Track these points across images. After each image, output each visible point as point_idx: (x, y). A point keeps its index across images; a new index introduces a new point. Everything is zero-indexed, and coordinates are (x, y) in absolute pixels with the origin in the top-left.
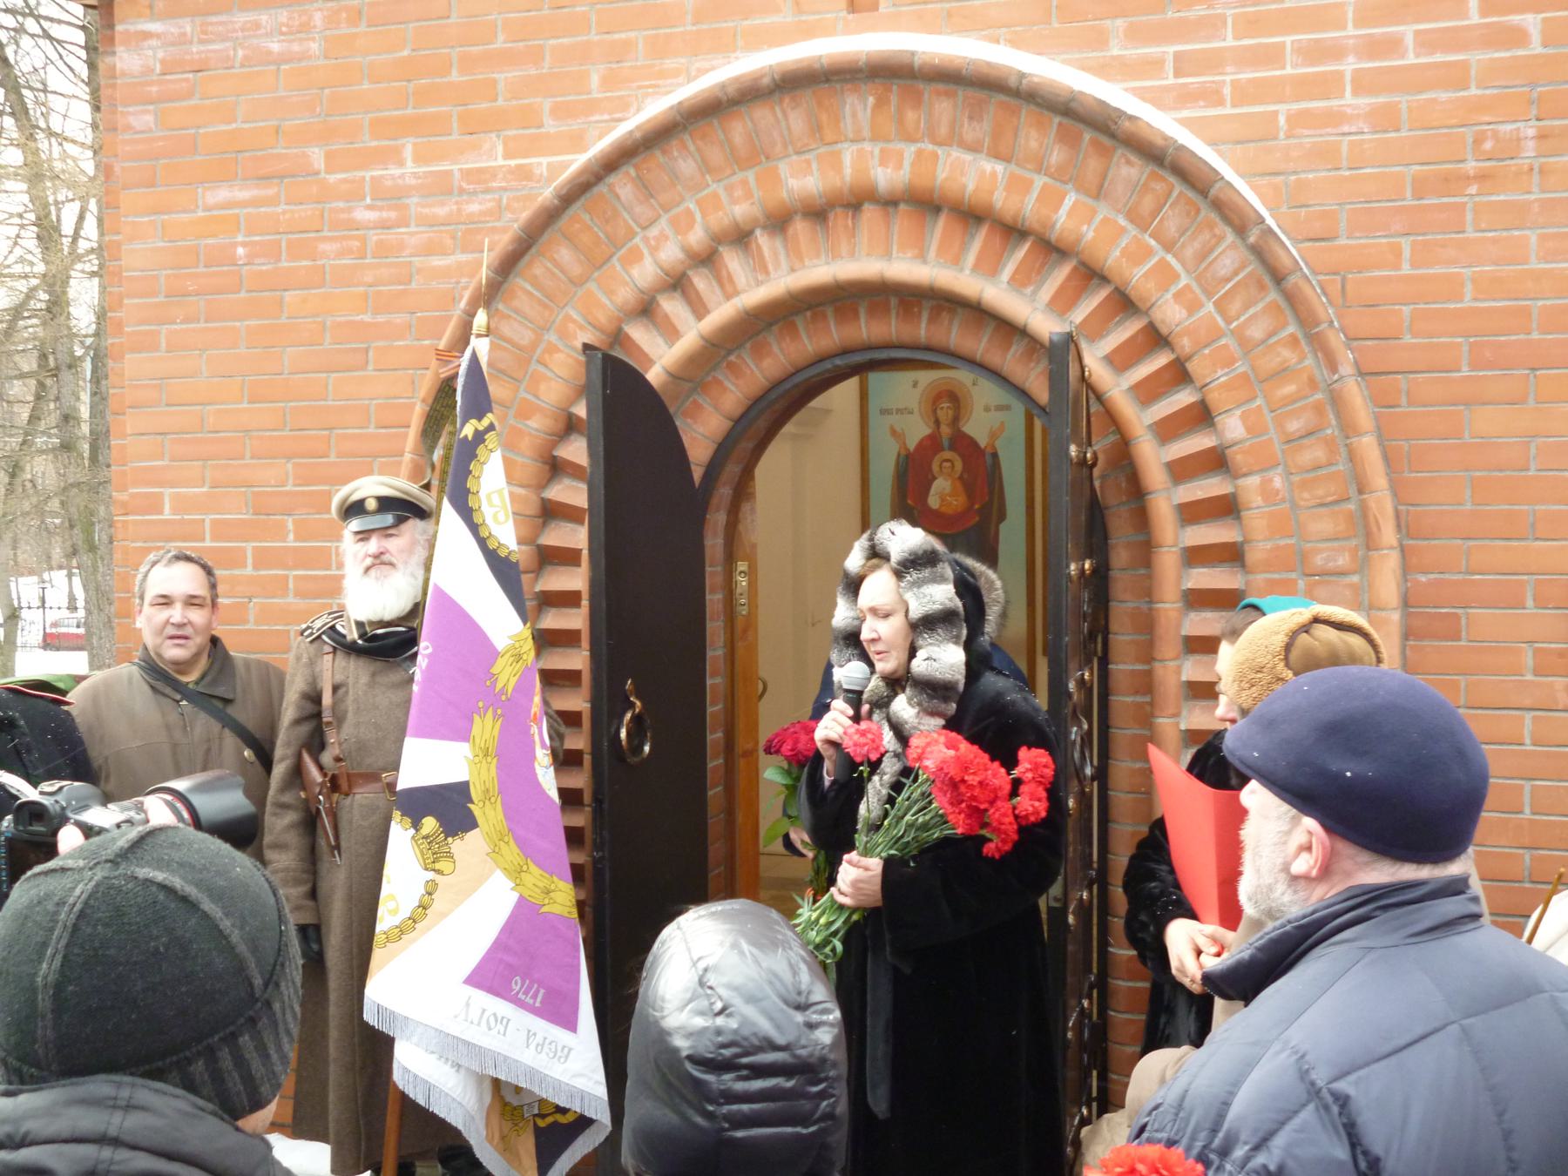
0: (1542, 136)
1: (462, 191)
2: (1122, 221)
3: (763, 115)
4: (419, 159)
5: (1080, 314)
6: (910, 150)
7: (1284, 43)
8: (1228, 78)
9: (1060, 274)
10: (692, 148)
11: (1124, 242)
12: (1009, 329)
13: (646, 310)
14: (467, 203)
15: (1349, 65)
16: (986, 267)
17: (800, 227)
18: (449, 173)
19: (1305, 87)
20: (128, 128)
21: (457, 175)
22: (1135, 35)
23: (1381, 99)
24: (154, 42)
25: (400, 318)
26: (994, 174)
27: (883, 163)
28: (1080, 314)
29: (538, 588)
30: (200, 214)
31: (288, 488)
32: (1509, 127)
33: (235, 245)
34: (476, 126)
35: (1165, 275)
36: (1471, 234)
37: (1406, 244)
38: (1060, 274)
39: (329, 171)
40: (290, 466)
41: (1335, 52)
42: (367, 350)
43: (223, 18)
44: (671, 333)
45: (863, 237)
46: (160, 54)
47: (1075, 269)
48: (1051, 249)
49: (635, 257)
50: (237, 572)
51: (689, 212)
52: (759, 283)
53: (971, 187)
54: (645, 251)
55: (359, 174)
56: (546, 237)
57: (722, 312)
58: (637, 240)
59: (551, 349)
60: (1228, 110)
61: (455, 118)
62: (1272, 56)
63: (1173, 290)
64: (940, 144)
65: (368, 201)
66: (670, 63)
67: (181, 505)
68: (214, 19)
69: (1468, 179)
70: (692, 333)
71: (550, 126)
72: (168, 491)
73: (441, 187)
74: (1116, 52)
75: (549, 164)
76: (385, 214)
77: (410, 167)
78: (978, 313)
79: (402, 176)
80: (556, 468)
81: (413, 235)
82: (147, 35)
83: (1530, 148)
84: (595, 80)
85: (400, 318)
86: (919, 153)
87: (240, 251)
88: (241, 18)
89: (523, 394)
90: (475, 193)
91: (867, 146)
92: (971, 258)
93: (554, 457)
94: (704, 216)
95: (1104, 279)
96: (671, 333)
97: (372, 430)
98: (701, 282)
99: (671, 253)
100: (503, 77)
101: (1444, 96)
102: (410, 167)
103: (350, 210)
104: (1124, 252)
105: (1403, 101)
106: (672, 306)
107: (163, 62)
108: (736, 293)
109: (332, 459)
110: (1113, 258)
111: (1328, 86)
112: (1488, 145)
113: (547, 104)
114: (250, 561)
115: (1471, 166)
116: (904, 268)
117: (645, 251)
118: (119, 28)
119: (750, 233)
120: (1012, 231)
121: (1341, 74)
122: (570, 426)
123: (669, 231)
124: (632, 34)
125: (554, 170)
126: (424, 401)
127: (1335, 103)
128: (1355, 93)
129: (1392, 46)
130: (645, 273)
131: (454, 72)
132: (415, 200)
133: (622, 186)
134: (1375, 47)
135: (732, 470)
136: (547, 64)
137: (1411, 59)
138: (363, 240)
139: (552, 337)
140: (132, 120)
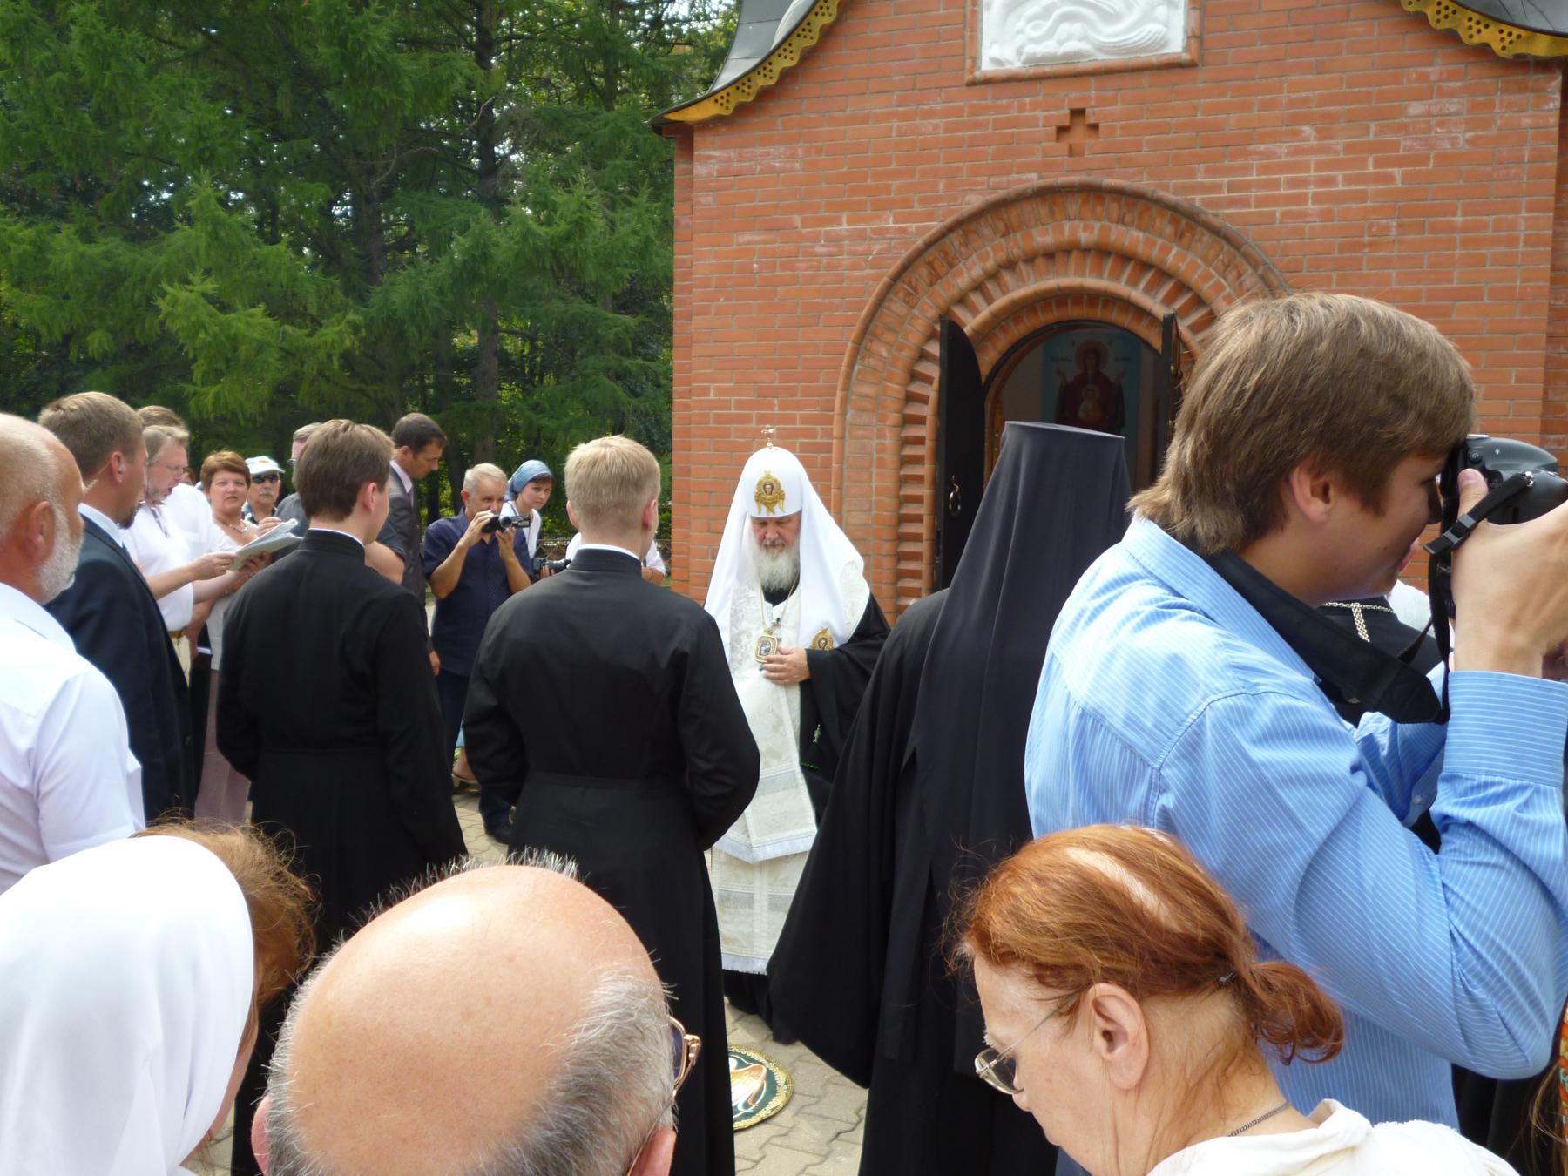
0: (1400, 226)
1: (871, 239)
2: (1199, 261)
3: (1027, 209)
4: (850, 222)
5: (1177, 305)
6: (1097, 225)
7: (1280, 179)
8: (1253, 194)
9: (1168, 287)
10: (990, 220)
11: (1200, 271)
12: (1142, 313)
13: (962, 300)
14: (874, 244)
15: (1311, 190)
16: (1133, 282)
17: (1040, 261)
18: (865, 230)
19: (1290, 200)
20: (699, 203)
21: (869, 230)
22: (1210, 172)
23: (1325, 206)
24: (713, 161)
25: (836, 301)
26: (1138, 237)
27: (1084, 231)
28: (1177, 305)
29: (902, 435)
30: (735, 247)
31: (777, 384)
32: (1384, 221)
33: (753, 263)
34: (879, 207)
35: (1219, 288)
36: (1364, 271)
37: (1334, 275)
38: (1168, 287)
39: (803, 227)
40: (777, 373)
41: (1304, 183)
42: (819, 318)
43: (751, 149)
44: (974, 311)
45: (1072, 266)
46: (717, 167)
47: (1175, 284)
48: (1163, 274)
49: (960, 273)
50: (747, 426)
51: (987, 252)
52: (1019, 287)
53: (1127, 243)
54: (964, 270)
56: (916, 263)
57: (1000, 302)
58: (961, 265)
59: (915, 317)
60: (1253, 210)
61: (869, 203)
63: (1223, 294)
64: (1111, 222)
65: (823, 242)
66: (979, 179)
67: (719, 391)
68: (746, 150)
69: (1362, 245)
70: (985, 312)
71: (917, 208)
72: (713, 386)
73: (861, 236)
74: (1199, 180)
75: (916, 227)
76: (831, 249)
77: (845, 227)
78: (1127, 305)
79: (841, 230)
80: (914, 376)
81: (845, 259)
82: (710, 157)
83: (1394, 232)
84: (941, 186)
85: (836, 301)
86: (1102, 228)
87: (755, 266)
88: (760, 150)
89: (900, 339)
90: (877, 239)
91: (1077, 222)
92: (1125, 277)
93: (913, 371)
94: (995, 254)
95: (1189, 289)
96: (974, 311)
97: (820, 356)
98: (991, 287)
99: (977, 272)
100: (895, 184)
101: (1355, 205)
102: (845, 227)
103: (812, 247)
104: (1199, 276)
105: (1336, 207)
106: (976, 298)
107: (718, 171)
108: (1008, 292)
109: (799, 370)
110: (1194, 279)
111: (1301, 199)
112: (1374, 229)
113: (916, 197)
114: (754, 419)
115: (1366, 238)
116: (1091, 282)
117: (964, 270)
118: (696, 153)
119: (1017, 262)
120: (1145, 266)
121: (1306, 195)
122: (923, 356)
123: (977, 261)
124: (961, 164)
125: (920, 231)
126: (853, 342)
127: (1303, 208)
128: (1314, 203)
129: (1331, 181)
130: (963, 282)
131: (869, 180)
132: (847, 242)
133: (955, 240)
135: (997, 380)
136: (917, 177)
137: (1340, 188)
138: (819, 262)
139: (916, 311)
140: (702, 200)
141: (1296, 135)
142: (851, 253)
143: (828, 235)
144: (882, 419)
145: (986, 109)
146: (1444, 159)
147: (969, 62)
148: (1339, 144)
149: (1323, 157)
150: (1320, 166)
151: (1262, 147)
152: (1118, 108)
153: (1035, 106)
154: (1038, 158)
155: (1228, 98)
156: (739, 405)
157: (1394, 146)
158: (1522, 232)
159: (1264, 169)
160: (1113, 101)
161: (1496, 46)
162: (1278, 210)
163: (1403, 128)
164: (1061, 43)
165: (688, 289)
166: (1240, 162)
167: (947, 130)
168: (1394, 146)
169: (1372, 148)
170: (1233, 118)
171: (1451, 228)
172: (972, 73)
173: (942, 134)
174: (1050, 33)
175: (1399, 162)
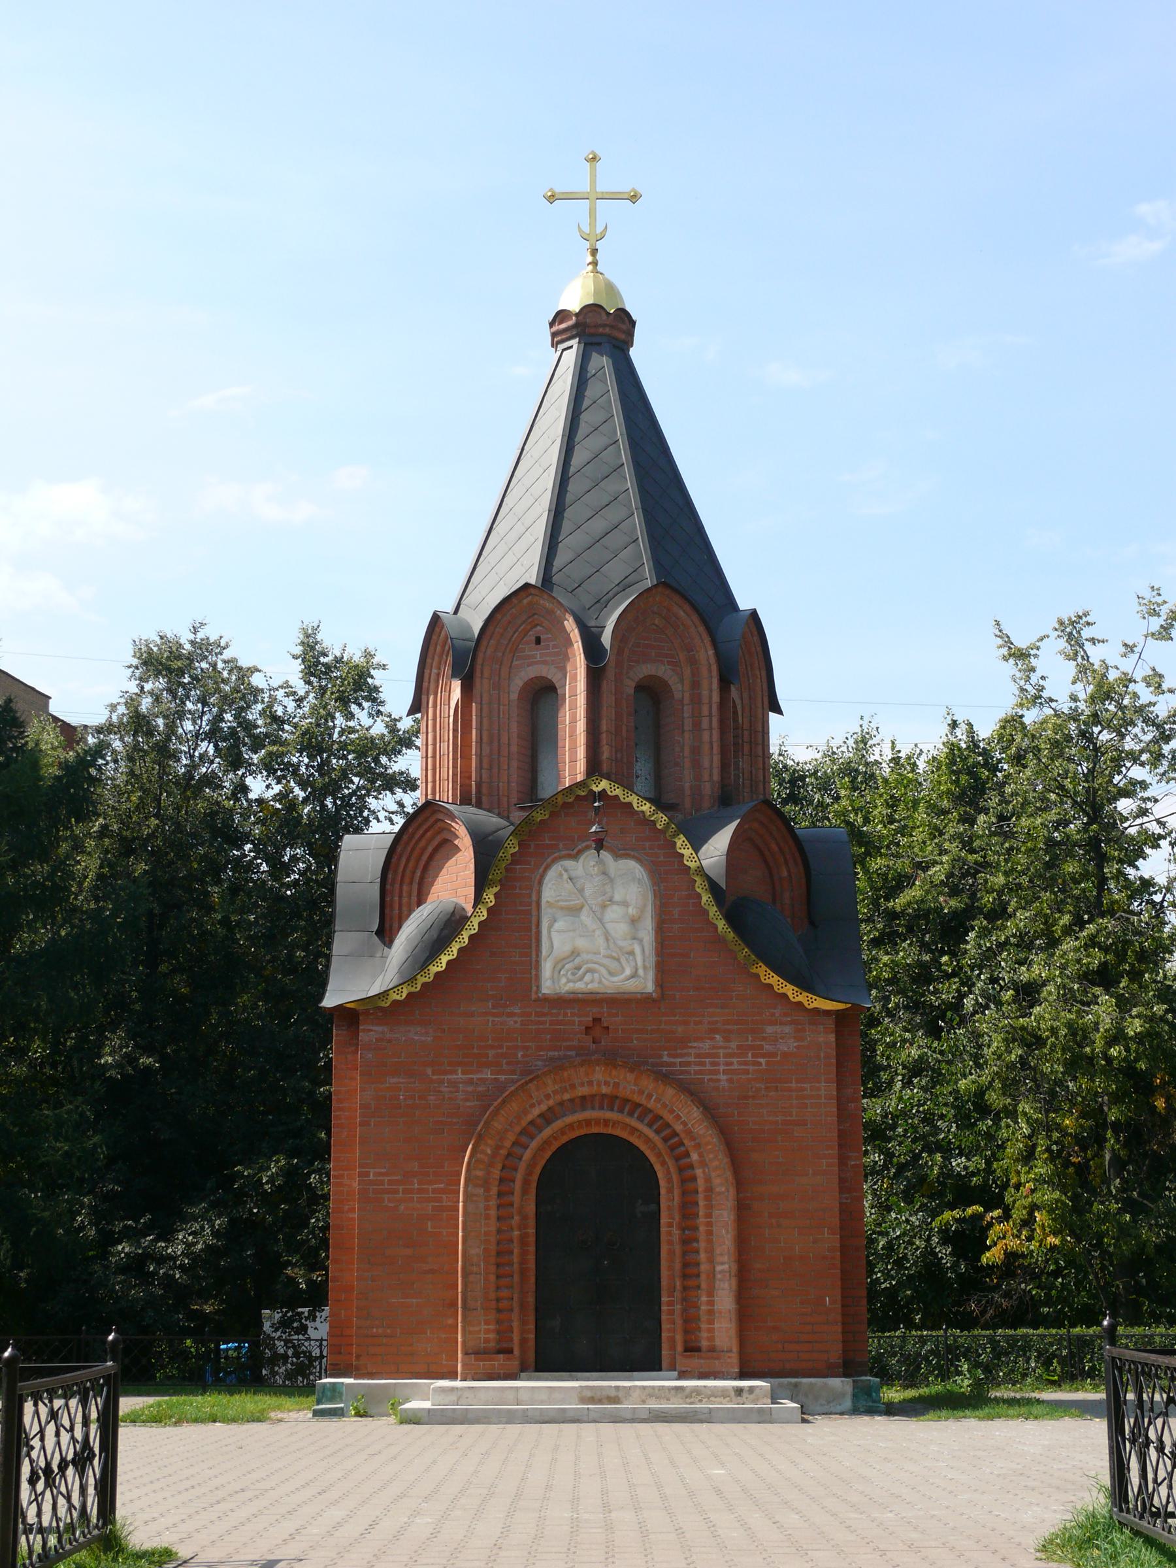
39: (433, 1074)
55: (442, 1077)
62: (703, 1064)
67: (375, 1174)
71: (505, 1067)
73: (470, 1081)
81: (460, 1095)
82: (372, 1030)
100: (491, 1053)
102: (460, 1076)
105: (735, 1077)
115: (750, 1094)
118: (361, 1027)
129: (731, 1064)
134: (727, 1064)
141: (713, 1039)
142: (463, 1091)
143: (449, 1081)
144: (487, 1190)
145: (544, 1015)
146: (785, 1055)
147: (534, 988)
148: (733, 1045)
149: (725, 1051)
150: (726, 1056)
151: (695, 1044)
152: (619, 1019)
153: (573, 1015)
154: (575, 1043)
155: (677, 1018)
156: (390, 1182)
157: (761, 1047)
158: (823, 1092)
159: (698, 1056)
160: (616, 1015)
161: (806, 1004)
162: (707, 1077)
163: (764, 1039)
164: (587, 984)
165: (339, 1109)
166: (685, 1051)
167: (521, 1025)
168: (761, 1047)
169: (751, 1047)
170: (680, 1029)
171: (790, 1089)
172: (537, 992)
173: (518, 1026)
174: (581, 979)
175: (763, 1056)
